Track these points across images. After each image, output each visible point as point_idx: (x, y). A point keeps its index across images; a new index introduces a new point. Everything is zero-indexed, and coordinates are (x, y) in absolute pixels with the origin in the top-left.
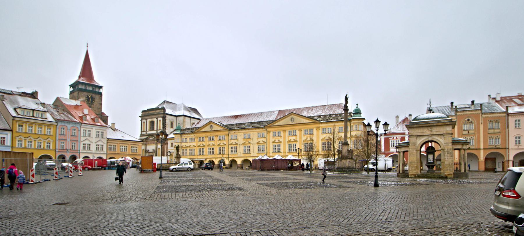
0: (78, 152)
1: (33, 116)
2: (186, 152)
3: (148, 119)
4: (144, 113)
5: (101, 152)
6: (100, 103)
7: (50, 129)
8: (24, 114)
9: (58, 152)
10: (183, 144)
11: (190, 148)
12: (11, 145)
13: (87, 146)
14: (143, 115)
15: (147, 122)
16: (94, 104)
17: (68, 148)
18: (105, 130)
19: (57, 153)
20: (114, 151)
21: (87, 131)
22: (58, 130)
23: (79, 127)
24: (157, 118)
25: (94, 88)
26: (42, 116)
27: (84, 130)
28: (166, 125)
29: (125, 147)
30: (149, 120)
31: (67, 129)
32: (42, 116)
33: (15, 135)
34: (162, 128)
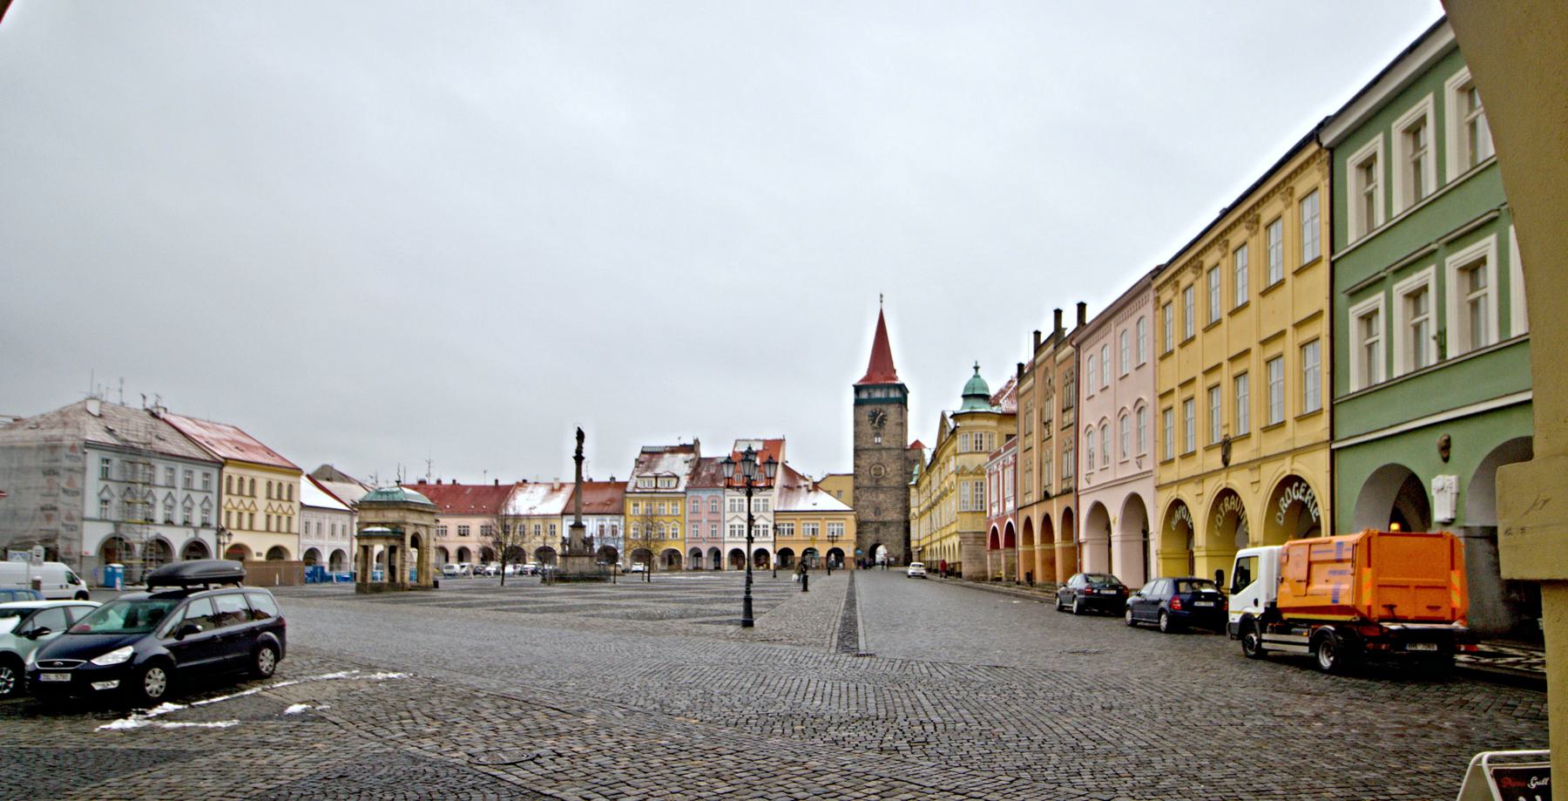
0: (720, 542)
1: (656, 487)
5: (764, 540)
7: (677, 505)
9: (689, 543)
13: (737, 529)
16: (886, 427)
17: (704, 536)
18: (770, 495)
21: (737, 501)
23: (722, 496)
25: (885, 391)
27: (731, 500)
29: (788, 525)
33: (629, 519)
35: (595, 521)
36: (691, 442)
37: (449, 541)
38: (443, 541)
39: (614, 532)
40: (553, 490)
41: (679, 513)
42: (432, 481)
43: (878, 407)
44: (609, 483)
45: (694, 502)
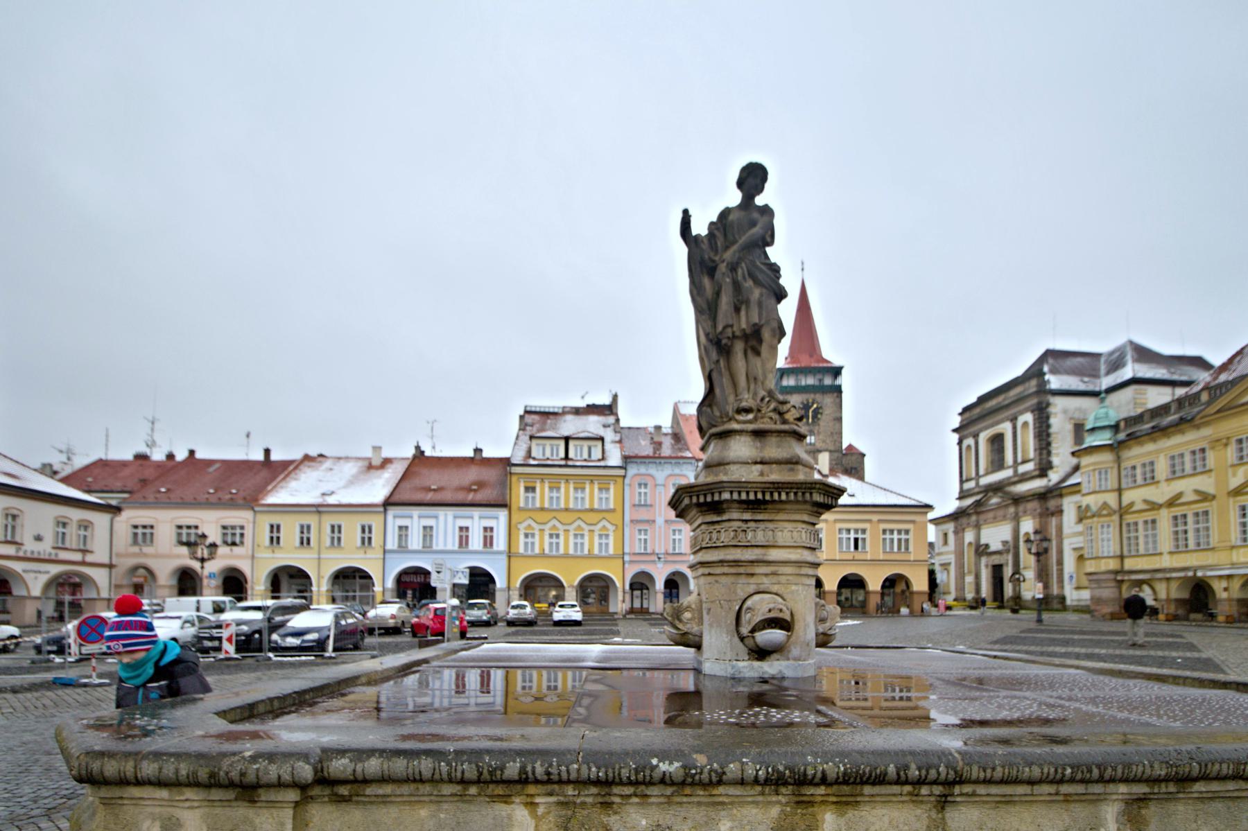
2: (1155, 536)
3: (981, 430)
4: (967, 415)
6: (837, 415)
8: (544, 455)
9: (631, 562)
10: (1128, 497)
11: (1178, 511)
12: (507, 550)
14: (965, 423)
15: (977, 443)
17: (660, 549)
19: (627, 565)
20: (903, 550)
22: (627, 488)
24: (1014, 420)
26: (590, 455)
28: (1051, 439)
30: (984, 437)
31: (656, 485)
32: (590, 455)
34: (1035, 450)
35: (450, 518)
36: (606, 400)
37: (157, 556)
38: (145, 555)
39: (488, 541)
40: (370, 467)
41: (612, 506)
42: (158, 456)
43: (811, 397)
44: (472, 459)
45: (640, 485)
